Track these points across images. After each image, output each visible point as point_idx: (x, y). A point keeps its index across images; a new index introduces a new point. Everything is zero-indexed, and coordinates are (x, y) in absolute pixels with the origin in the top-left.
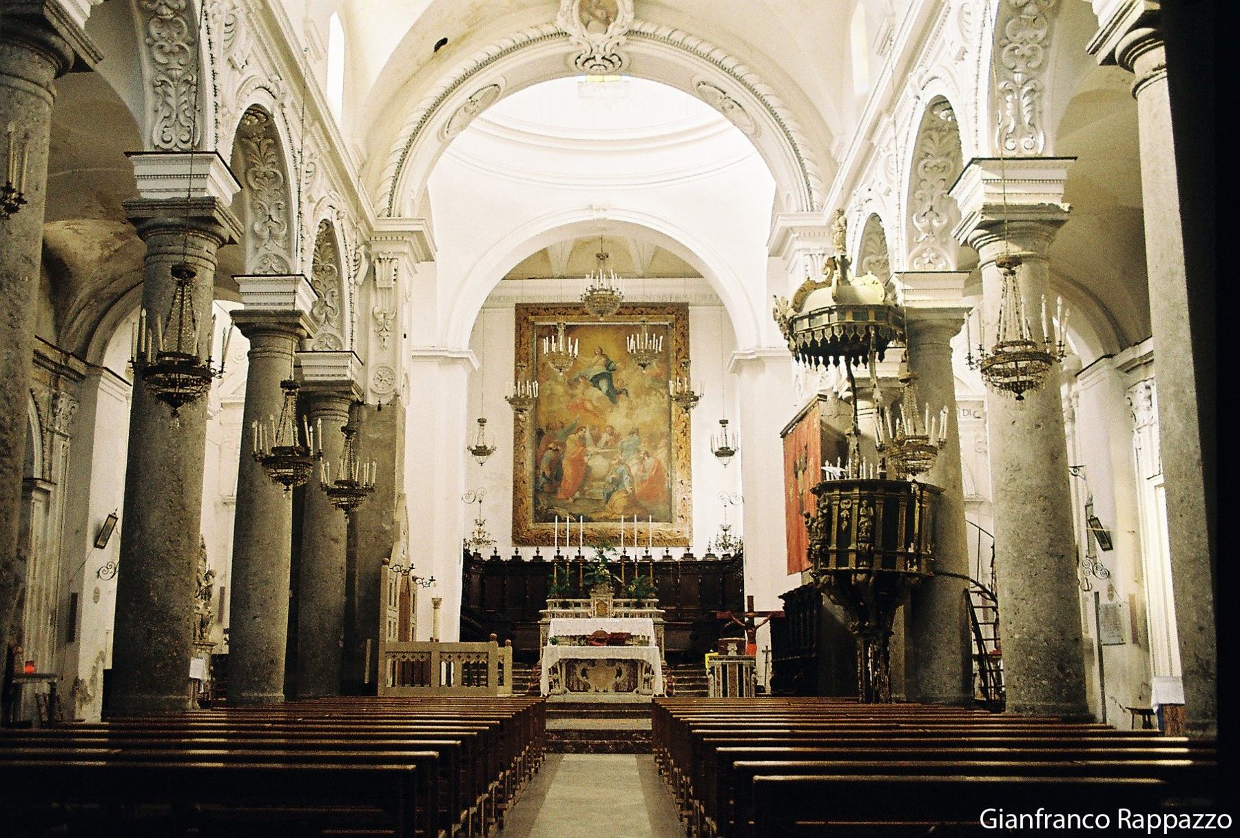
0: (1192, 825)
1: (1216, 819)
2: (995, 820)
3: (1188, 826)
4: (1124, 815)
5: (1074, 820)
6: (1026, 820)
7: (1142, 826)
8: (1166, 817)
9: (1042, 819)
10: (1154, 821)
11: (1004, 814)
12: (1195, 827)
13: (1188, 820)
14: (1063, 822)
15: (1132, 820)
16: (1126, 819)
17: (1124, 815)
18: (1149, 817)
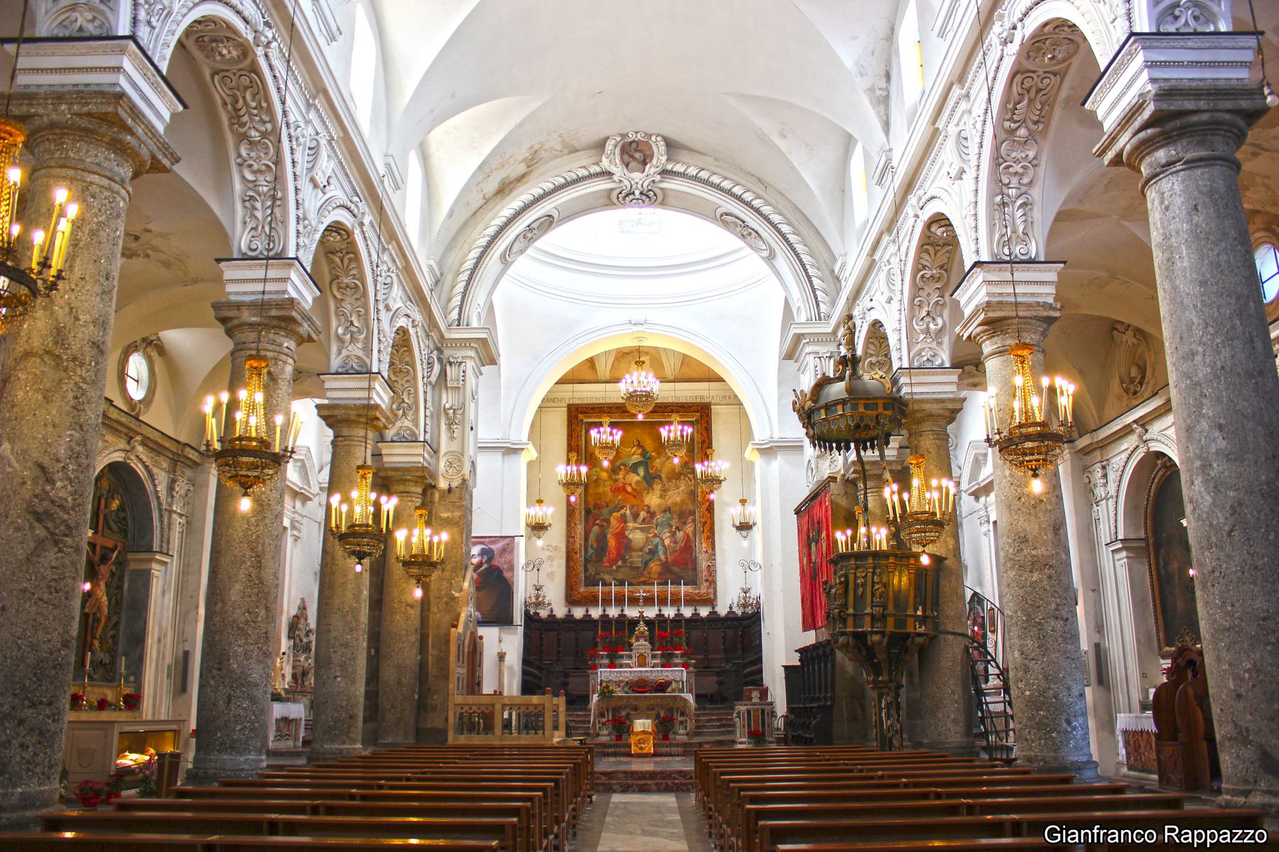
0: (1231, 839)
1: (1254, 834)
2: (1059, 835)
3: (1228, 840)
5: (1126, 834)
6: (1086, 834)
7: (1190, 840)
8: (1209, 832)
9: (1098, 834)
12: (1234, 841)
13: (1228, 836)
15: (1179, 836)
16: (1173, 834)
18: (1196, 832)
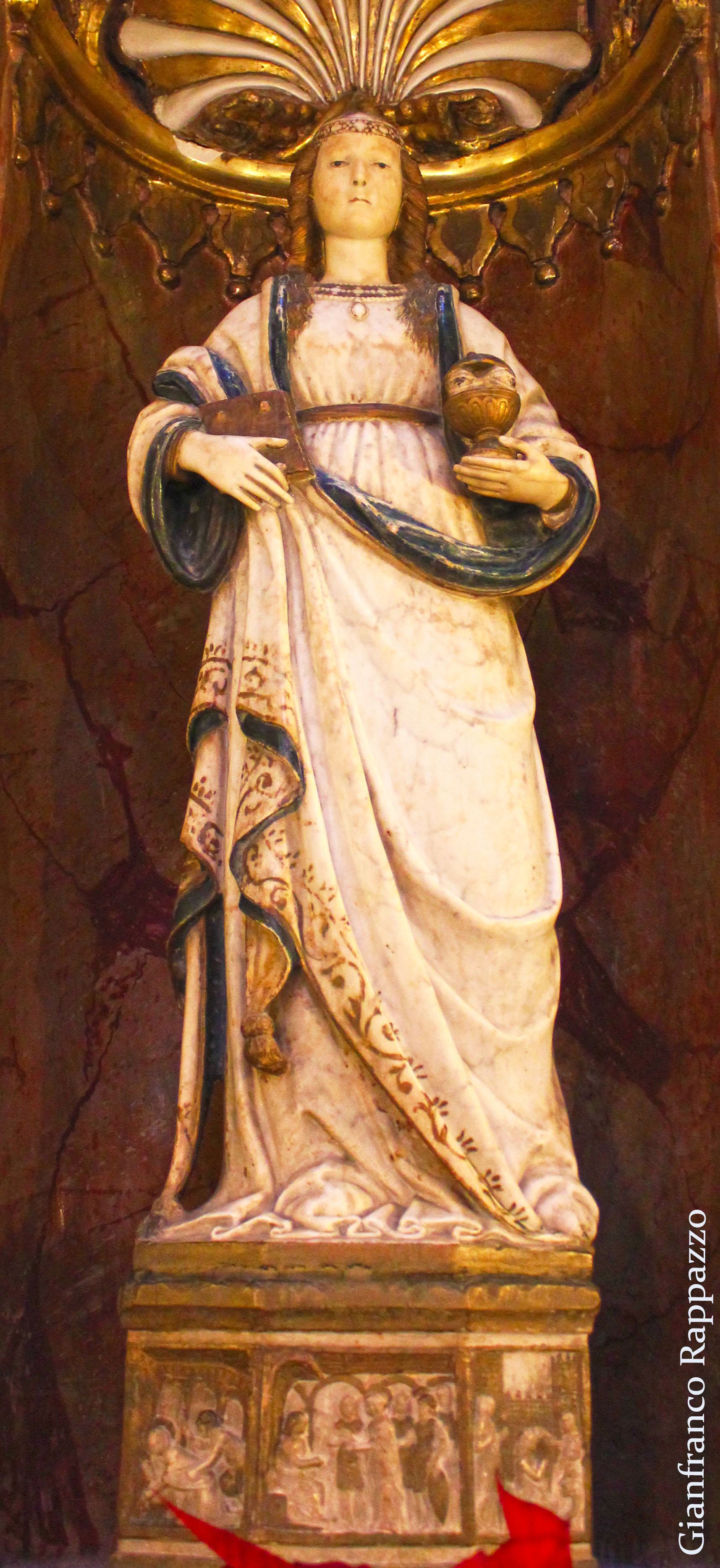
3: (703, 1269)
4: (687, 1355)
5: (695, 1424)
6: (694, 1490)
7: (703, 1330)
9: (694, 1468)
10: (697, 1314)
11: (686, 1520)
14: (698, 1443)
17: (687, 1355)
